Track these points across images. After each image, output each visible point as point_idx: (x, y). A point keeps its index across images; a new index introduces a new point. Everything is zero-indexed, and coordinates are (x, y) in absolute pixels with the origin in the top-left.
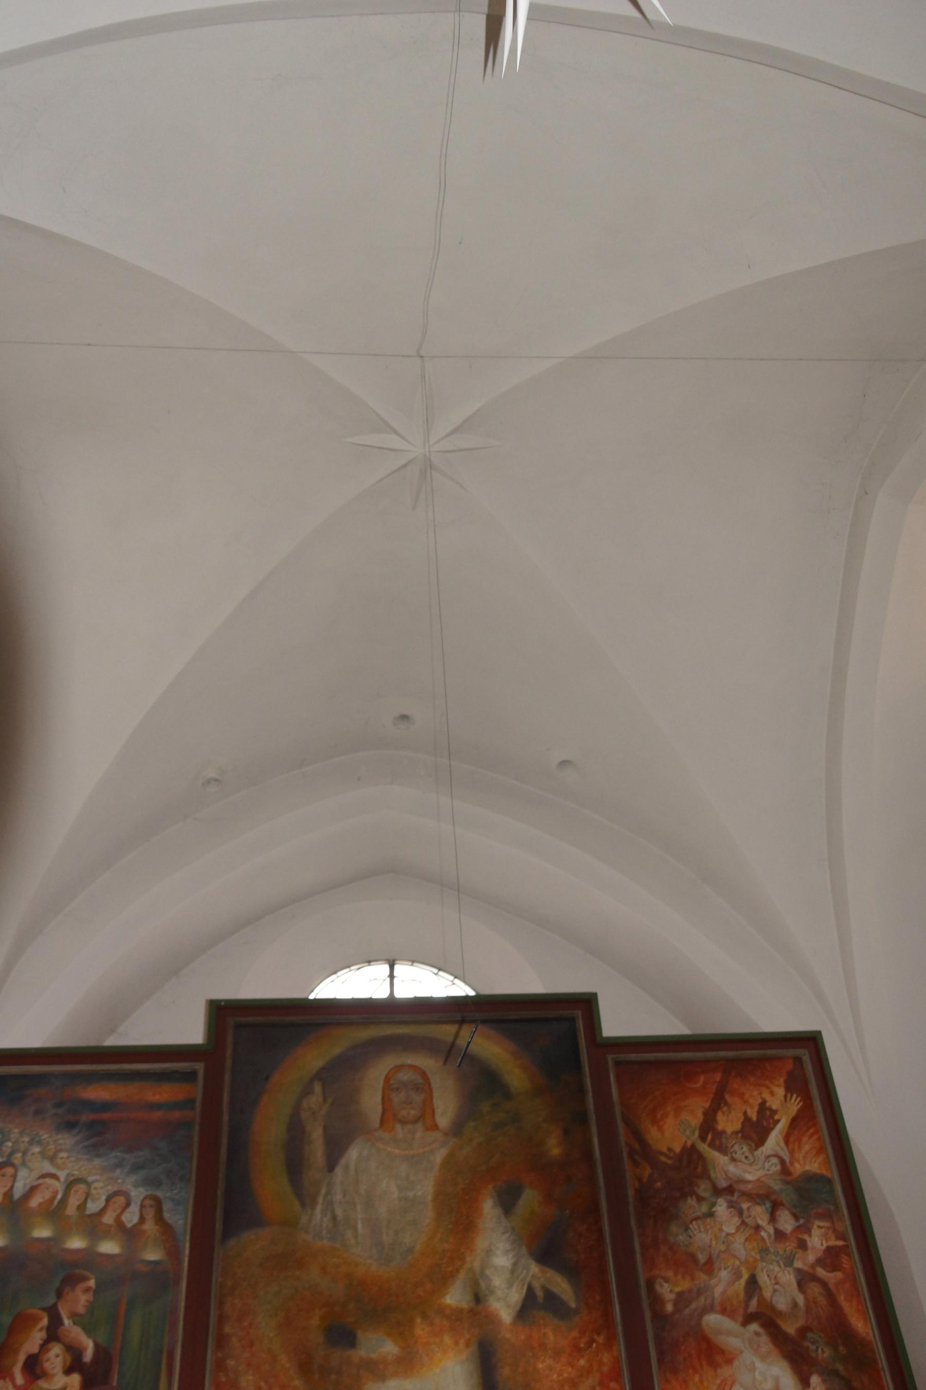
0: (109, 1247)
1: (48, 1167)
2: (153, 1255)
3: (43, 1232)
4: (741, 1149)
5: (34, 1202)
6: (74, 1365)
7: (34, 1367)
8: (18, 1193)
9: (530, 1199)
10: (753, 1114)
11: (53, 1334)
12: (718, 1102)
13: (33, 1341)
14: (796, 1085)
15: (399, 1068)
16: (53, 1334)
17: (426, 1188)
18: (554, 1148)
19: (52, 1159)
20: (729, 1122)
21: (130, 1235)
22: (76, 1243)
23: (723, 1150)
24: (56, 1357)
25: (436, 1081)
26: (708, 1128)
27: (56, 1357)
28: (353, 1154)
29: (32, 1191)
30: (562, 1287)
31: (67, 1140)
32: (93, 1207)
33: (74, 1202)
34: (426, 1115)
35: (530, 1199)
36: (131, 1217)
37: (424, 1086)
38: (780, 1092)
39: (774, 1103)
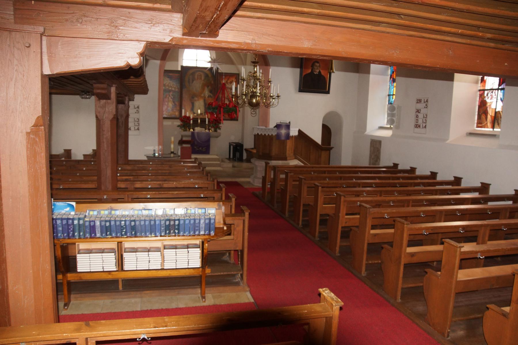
0: (173, 89)
1: (167, 81)
2: (177, 90)
3: (167, 87)
4: (229, 84)
5: (167, 84)
6: (171, 98)
7: (168, 98)
8: (165, 83)
9: (210, 87)
10: (231, 81)
11: (169, 95)
12: (228, 79)
13: (168, 96)
14: (236, 78)
15: (199, 73)
16: (169, 95)
17: (201, 85)
18: (212, 82)
19: (167, 81)
20: (229, 81)
21: (175, 88)
22: (170, 88)
23: (227, 84)
24: (170, 98)
25: (202, 75)
26: (227, 82)
27: (170, 98)
28: (194, 82)
29: (166, 84)
30: (211, 95)
31: (168, 79)
32: (171, 85)
33: (170, 85)
34: (201, 78)
35: (210, 87)
36: (175, 86)
37: (201, 76)
38: (234, 79)
39: (233, 80)
